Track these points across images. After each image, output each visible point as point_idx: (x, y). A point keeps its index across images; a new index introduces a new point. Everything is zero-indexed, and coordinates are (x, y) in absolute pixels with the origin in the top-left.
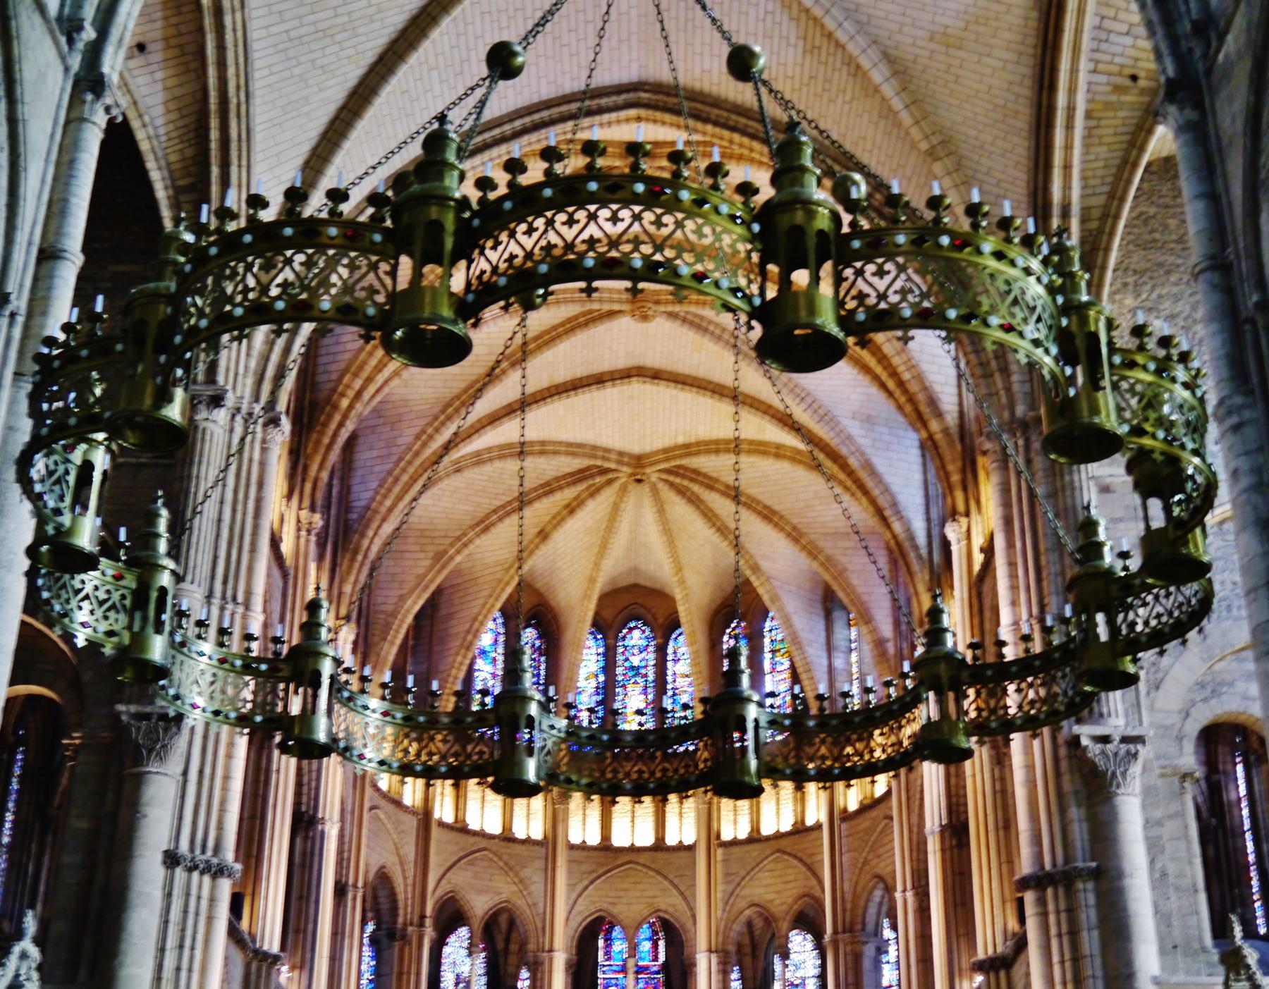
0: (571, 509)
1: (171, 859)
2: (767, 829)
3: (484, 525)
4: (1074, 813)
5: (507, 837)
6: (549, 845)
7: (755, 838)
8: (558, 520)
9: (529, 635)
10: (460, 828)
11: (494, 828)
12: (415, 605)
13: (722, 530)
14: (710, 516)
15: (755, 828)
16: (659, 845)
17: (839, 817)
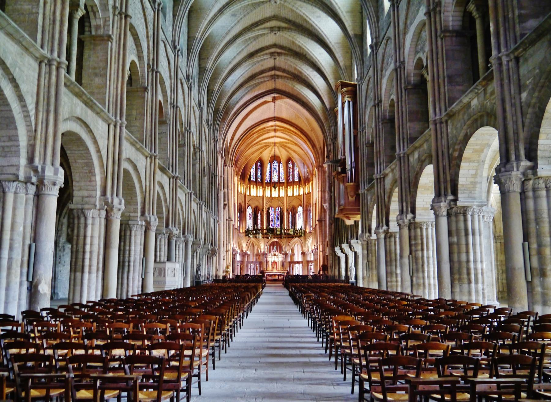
0: (265, 149)
1: (227, 220)
2: (295, 195)
3: (253, 153)
4: (323, 214)
5: (257, 196)
6: (263, 197)
7: (293, 196)
8: (263, 151)
9: (259, 163)
10: (250, 195)
11: (255, 195)
12: (243, 166)
13: (288, 152)
14: (286, 150)
15: (293, 194)
16: (279, 196)
17: (304, 194)
